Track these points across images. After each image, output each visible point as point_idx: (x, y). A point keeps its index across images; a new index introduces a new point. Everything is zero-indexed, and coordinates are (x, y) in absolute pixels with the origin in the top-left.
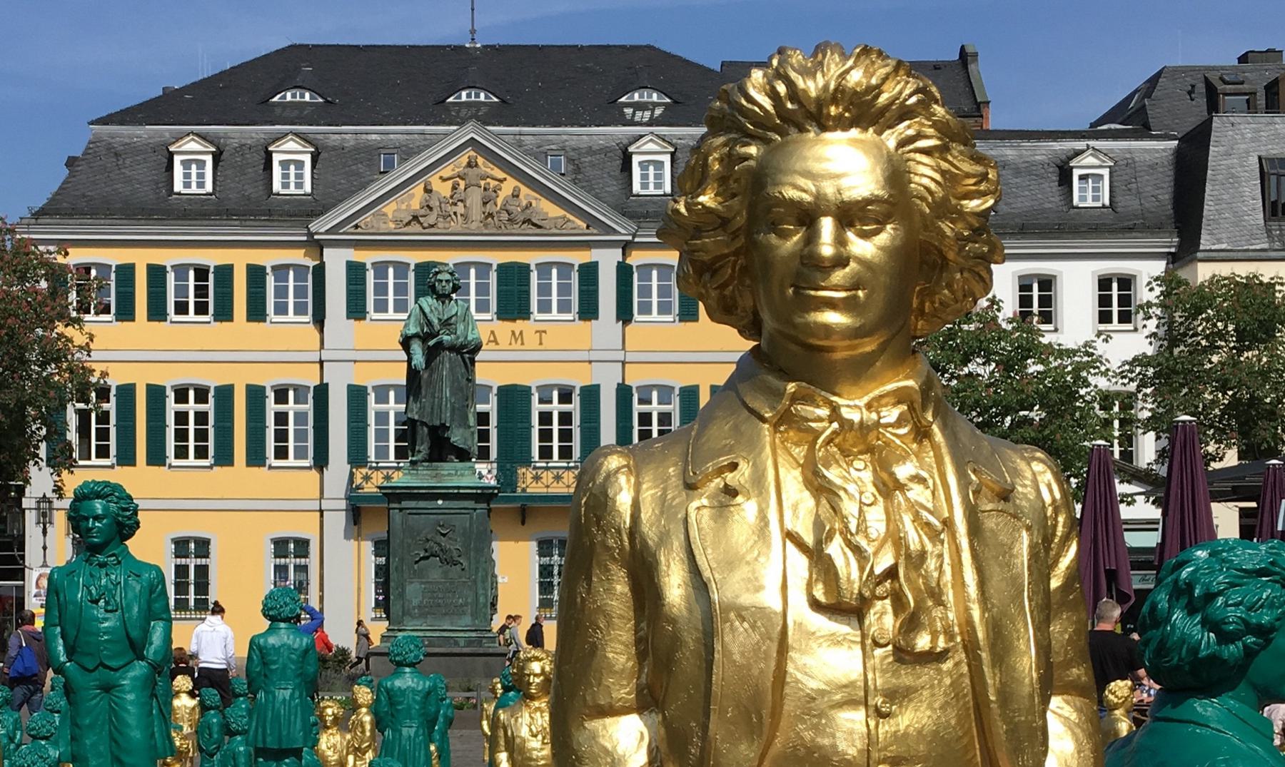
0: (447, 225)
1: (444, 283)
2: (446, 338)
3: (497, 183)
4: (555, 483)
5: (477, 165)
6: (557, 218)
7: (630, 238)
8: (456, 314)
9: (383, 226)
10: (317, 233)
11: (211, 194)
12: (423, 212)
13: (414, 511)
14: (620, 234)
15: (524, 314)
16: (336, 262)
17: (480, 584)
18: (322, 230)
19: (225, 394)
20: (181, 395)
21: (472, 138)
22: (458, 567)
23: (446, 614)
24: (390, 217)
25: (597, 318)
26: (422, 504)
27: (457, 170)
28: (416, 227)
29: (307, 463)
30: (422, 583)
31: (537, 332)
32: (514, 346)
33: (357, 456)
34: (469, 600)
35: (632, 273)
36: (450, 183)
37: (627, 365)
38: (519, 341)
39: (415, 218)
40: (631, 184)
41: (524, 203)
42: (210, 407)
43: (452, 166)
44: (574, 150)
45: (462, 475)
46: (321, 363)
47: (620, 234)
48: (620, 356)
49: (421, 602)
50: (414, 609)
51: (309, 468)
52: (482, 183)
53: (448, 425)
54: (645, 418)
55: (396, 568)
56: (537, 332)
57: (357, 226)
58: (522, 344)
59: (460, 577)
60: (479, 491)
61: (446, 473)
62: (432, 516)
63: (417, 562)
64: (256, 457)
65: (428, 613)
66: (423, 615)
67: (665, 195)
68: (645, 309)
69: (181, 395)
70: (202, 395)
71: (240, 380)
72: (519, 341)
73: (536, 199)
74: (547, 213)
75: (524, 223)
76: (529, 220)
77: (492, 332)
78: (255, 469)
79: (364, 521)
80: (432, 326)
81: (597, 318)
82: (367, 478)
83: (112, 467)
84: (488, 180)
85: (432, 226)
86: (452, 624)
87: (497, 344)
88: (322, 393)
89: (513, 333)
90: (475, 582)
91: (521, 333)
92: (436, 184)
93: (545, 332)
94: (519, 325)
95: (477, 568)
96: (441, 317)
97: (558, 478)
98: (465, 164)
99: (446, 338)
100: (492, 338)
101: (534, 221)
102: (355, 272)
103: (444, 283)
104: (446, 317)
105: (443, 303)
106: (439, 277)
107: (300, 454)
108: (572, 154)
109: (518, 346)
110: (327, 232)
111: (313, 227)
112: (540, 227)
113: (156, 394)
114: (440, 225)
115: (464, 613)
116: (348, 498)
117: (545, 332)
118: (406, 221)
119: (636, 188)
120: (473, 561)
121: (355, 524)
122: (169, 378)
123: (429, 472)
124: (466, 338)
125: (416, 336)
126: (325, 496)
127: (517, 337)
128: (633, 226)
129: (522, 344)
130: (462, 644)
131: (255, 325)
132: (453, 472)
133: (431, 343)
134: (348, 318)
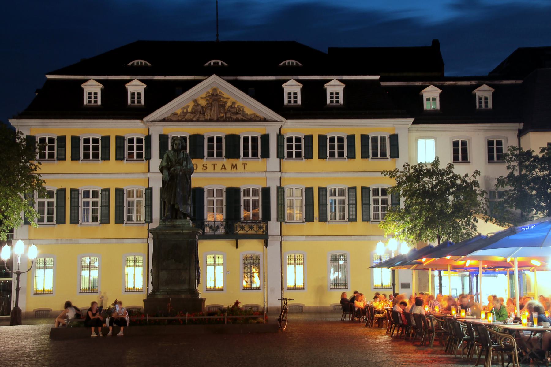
15: (237, 156)
31: (242, 164)
32: (233, 170)
38: (235, 168)
64: (119, 220)
70: (95, 194)
72: (235, 168)
73: (242, 107)
74: (247, 113)
77: (223, 165)
87: (225, 169)
89: (232, 165)
91: (236, 165)
93: (246, 164)
94: (234, 161)
97: (251, 228)
100: (223, 167)
109: (235, 170)
127: (234, 167)
129: (236, 169)
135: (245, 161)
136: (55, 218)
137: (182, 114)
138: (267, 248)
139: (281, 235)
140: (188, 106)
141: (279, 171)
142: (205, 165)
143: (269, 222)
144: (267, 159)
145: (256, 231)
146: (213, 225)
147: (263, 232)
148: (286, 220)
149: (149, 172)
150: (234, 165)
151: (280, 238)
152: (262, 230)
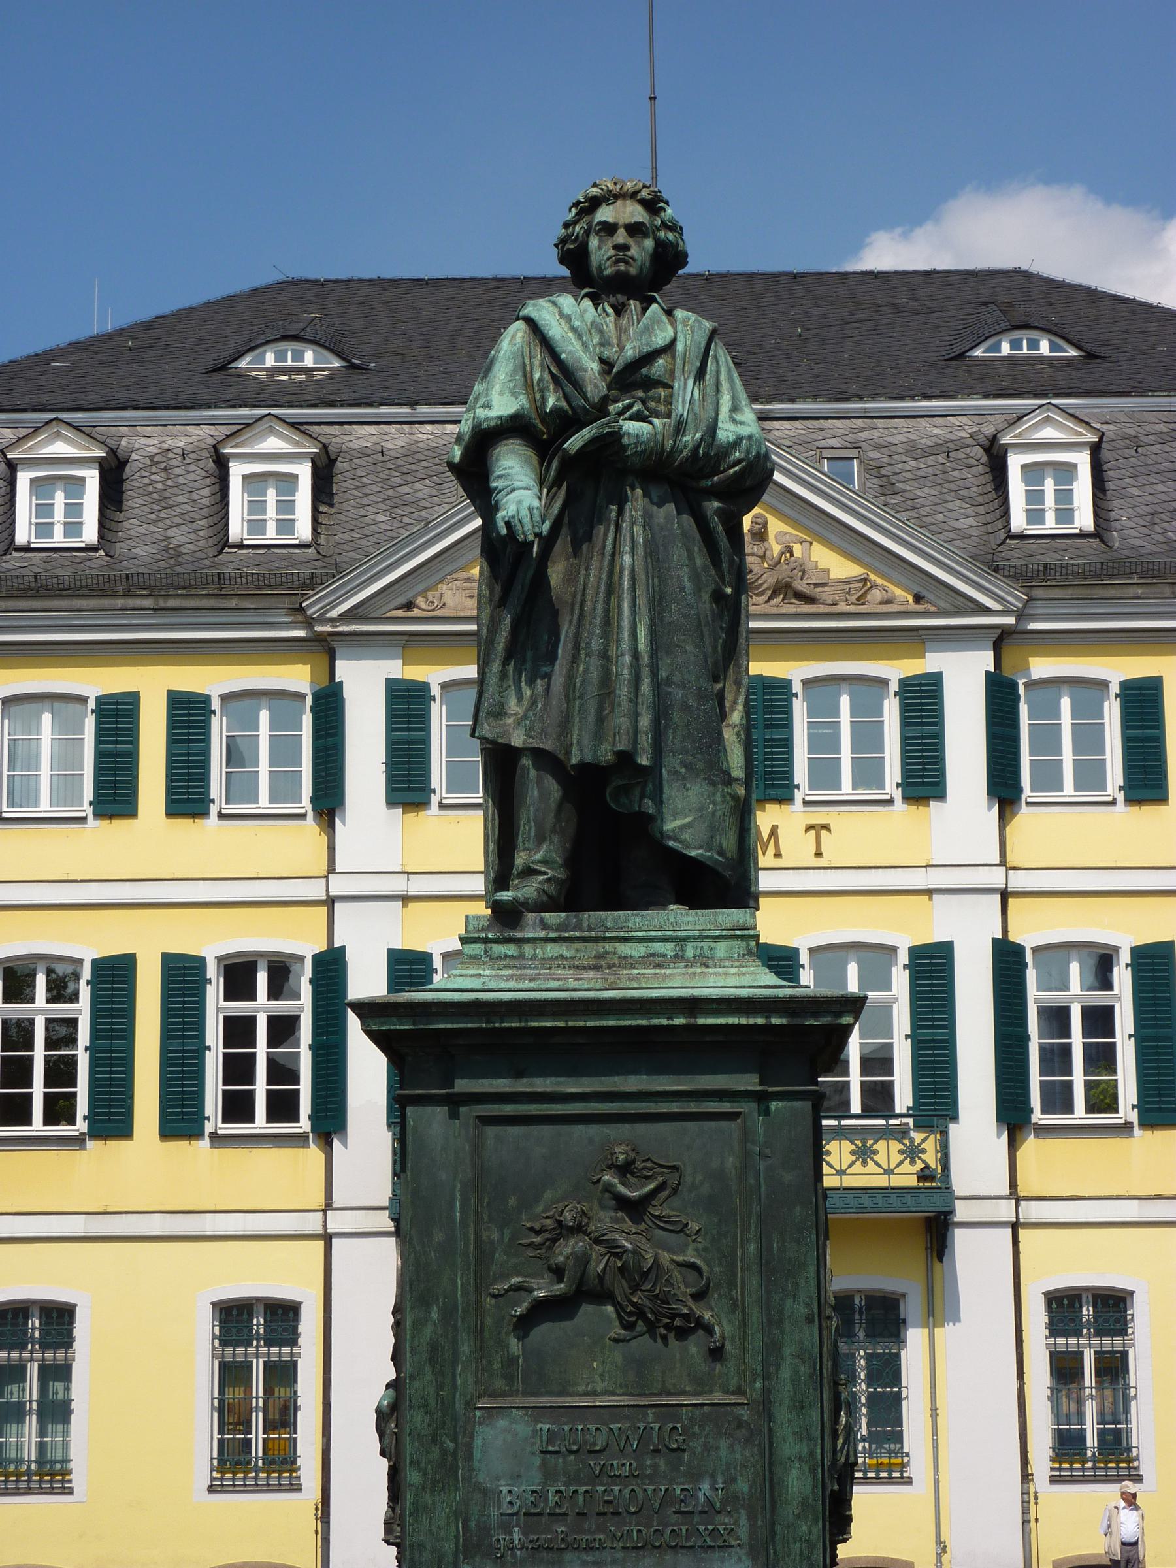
1: (621, 237)
2: (630, 427)
4: (858, 1167)
6: (848, 581)
7: (1011, 620)
8: (670, 346)
10: (323, 620)
11: (94, 549)
13: (508, 1109)
14: (986, 611)
17: (782, 1415)
18: (334, 613)
22: (694, 1347)
25: (941, 796)
29: (304, 1124)
30: (540, 1413)
31: (809, 828)
35: (1017, 698)
37: (1012, 902)
40: (1006, 514)
41: (776, 549)
44: (879, 447)
45: (705, 961)
47: (985, 610)
48: (996, 878)
49: (539, 1496)
53: (644, 761)
54: (1057, 1018)
55: (434, 1346)
56: (809, 828)
58: (778, 855)
59: (702, 1384)
60: (775, 1021)
61: (636, 950)
62: (580, 1130)
63: (524, 1325)
67: (1082, 535)
68: (1049, 777)
75: (775, 593)
76: (788, 586)
78: (182, 1145)
80: (577, 385)
81: (941, 796)
90: (765, 1408)
91: (774, 831)
93: (826, 827)
95: (773, 1349)
96: (610, 353)
97: (864, 1154)
99: (630, 427)
101: (801, 586)
103: (621, 237)
104: (630, 353)
105: (619, 310)
106: (605, 214)
108: (874, 454)
110: (345, 617)
111: (313, 605)
112: (811, 600)
117: (826, 827)
119: (1018, 521)
120: (755, 1317)
123: (566, 950)
124: (712, 429)
125: (514, 427)
126: (337, 1201)
128: (1016, 598)
129: (778, 855)
132: (668, 948)
133: (575, 442)
134: (391, 803)
135: (819, 816)
138: (941, 1260)
139: (1014, 1194)
141: (998, 862)
143: (953, 1128)
144: (933, 803)
145: (889, 1172)
147: (925, 1175)
148: (1037, 1116)
149: (331, 869)
150: (765, 834)
151: (1005, 1211)
152: (919, 1165)
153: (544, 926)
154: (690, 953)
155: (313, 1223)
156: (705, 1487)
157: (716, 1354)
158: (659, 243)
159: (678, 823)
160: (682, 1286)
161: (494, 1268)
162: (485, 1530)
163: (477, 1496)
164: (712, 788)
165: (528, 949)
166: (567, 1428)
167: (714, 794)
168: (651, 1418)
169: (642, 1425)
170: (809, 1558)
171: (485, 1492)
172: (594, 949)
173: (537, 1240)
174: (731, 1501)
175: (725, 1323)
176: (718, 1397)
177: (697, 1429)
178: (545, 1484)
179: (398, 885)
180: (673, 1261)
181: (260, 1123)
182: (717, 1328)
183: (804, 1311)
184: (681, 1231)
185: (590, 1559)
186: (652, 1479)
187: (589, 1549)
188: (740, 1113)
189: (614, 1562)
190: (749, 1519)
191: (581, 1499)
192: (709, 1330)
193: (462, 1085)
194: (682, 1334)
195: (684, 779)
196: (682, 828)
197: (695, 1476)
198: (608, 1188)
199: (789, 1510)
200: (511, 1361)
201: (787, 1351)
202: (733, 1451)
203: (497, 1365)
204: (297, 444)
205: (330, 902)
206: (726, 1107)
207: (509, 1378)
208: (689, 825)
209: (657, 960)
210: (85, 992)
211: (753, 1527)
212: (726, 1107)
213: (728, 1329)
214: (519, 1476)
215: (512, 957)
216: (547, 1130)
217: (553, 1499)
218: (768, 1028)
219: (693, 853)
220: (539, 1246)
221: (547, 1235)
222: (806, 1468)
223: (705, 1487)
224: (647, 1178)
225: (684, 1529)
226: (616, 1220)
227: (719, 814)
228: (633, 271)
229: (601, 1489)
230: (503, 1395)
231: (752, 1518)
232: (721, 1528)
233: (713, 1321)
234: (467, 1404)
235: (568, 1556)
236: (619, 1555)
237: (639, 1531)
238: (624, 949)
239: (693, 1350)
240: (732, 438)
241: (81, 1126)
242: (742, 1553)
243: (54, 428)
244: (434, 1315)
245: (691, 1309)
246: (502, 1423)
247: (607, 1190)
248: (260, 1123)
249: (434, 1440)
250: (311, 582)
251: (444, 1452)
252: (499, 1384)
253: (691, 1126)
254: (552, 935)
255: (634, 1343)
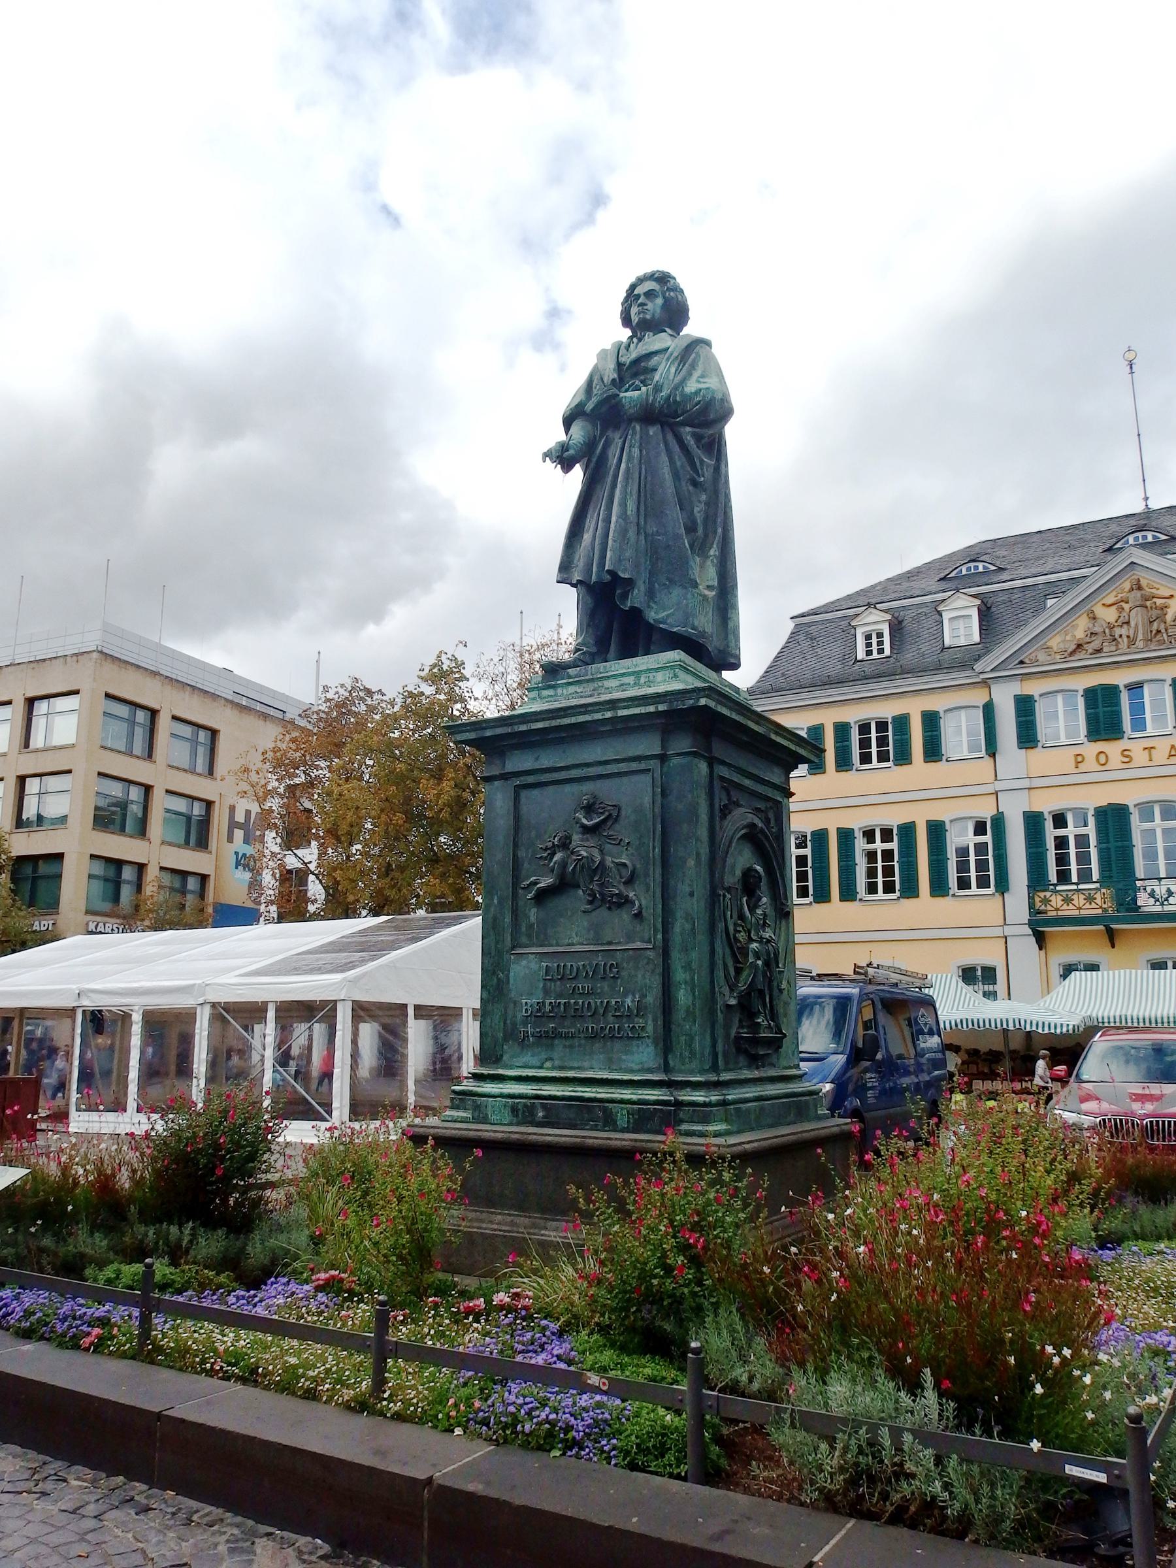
0: (1114, 648)
3: (1163, 601)
5: (1140, 588)
9: (1049, 658)
12: (1088, 639)
16: (1004, 698)
17: (676, 956)
18: (988, 669)
19: (908, 830)
20: (869, 835)
21: (1132, 563)
22: (625, 916)
23: (594, 1037)
24: (1055, 649)
26: (548, 759)
27: (1120, 595)
28: (1082, 655)
29: (992, 890)
33: (1037, 880)
34: (650, 999)
36: (1114, 607)
39: (1079, 646)
42: (894, 845)
43: (1114, 593)
46: (996, 793)
49: (541, 1005)
50: (525, 1025)
51: (993, 894)
52: (1148, 603)
55: (495, 919)
57: (1022, 662)
60: (661, 708)
62: (568, 788)
65: (556, 1035)
66: (546, 1039)
69: (869, 835)
70: (887, 835)
71: (920, 816)
79: (1049, 944)
82: (1046, 901)
83: (810, 904)
84: (1155, 600)
85: (1099, 651)
86: (610, 1065)
88: (999, 822)
92: (1100, 611)
98: (1127, 586)
102: (1025, 707)
107: (983, 883)
110: (992, 670)
111: (978, 667)
113: (846, 836)
114: (1105, 649)
115: (636, 1036)
116: (1031, 923)
118: (1070, 650)
121: (1040, 949)
122: (857, 821)
130: (622, 1120)
131: (932, 766)
136: (811, 891)
137: (1062, 646)
140: (1075, 627)
142: (1126, 753)
146: (1157, 889)
153: (570, 677)
154: (642, 680)
155: (998, 932)
156: (628, 1001)
157: (638, 916)
158: (664, 297)
159: (666, 613)
160: (618, 877)
161: (524, 872)
162: (514, 1024)
163: (512, 1005)
164: (684, 591)
165: (559, 691)
166: (555, 965)
167: (686, 594)
168: (600, 958)
169: (595, 963)
170: (690, 1046)
171: (515, 1003)
172: (591, 686)
173: (545, 855)
174: (641, 1009)
175: (642, 899)
176: (638, 945)
177: (625, 965)
178: (544, 998)
179: (1026, 783)
180: (613, 862)
181: (974, 890)
182: (637, 903)
183: (688, 889)
184: (619, 844)
185: (567, 1044)
186: (600, 995)
187: (566, 1038)
188: (649, 770)
189: (580, 1046)
190: (653, 1021)
191: (562, 1006)
192: (633, 903)
193: (510, 767)
194: (619, 905)
195: (668, 588)
196: (668, 616)
197: (625, 995)
198: (578, 821)
199: (679, 1015)
200: (531, 926)
201: (679, 914)
202: (645, 978)
203: (524, 929)
204: (972, 602)
205: (996, 793)
206: (643, 766)
207: (529, 936)
208: (672, 614)
209: (624, 687)
210: (895, 838)
211: (655, 1026)
212: (643, 766)
213: (644, 902)
214: (532, 994)
215: (551, 696)
216: (551, 789)
217: (548, 1008)
218: (658, 714)
219: (675, 630)
220: (546, 858)
221: (549, 851)
222: (689, 988)
223: (628, 1001)
224: (601, 813)
225: (616, 1026)
226: (582, 840)
227: (690, 605)
228: (648, 317)
229: (572, 1001)
230: (526, 946)
231: (655, 1020)
232: (637, 1026)
233: (634, 898)
234: (507, 952)
235: (556, 1042)
236: (583, 1042)
237: (592, 1027)
238: (607, 684)
239: (625, 916)
240: (693, 390)
241: (898, 894)
242: (649, 1041)
243: (871, 610)
244: (496, 901)
245: (620, 891)
246: (524, 963)
247: (577, 823)
248: (974, 890)
249: (494, 973)
250: (979, 658)
251: (499, 980)
252: (524, 940)
253: (625, 780)
254: (571, 680)
255: (594, 914)
